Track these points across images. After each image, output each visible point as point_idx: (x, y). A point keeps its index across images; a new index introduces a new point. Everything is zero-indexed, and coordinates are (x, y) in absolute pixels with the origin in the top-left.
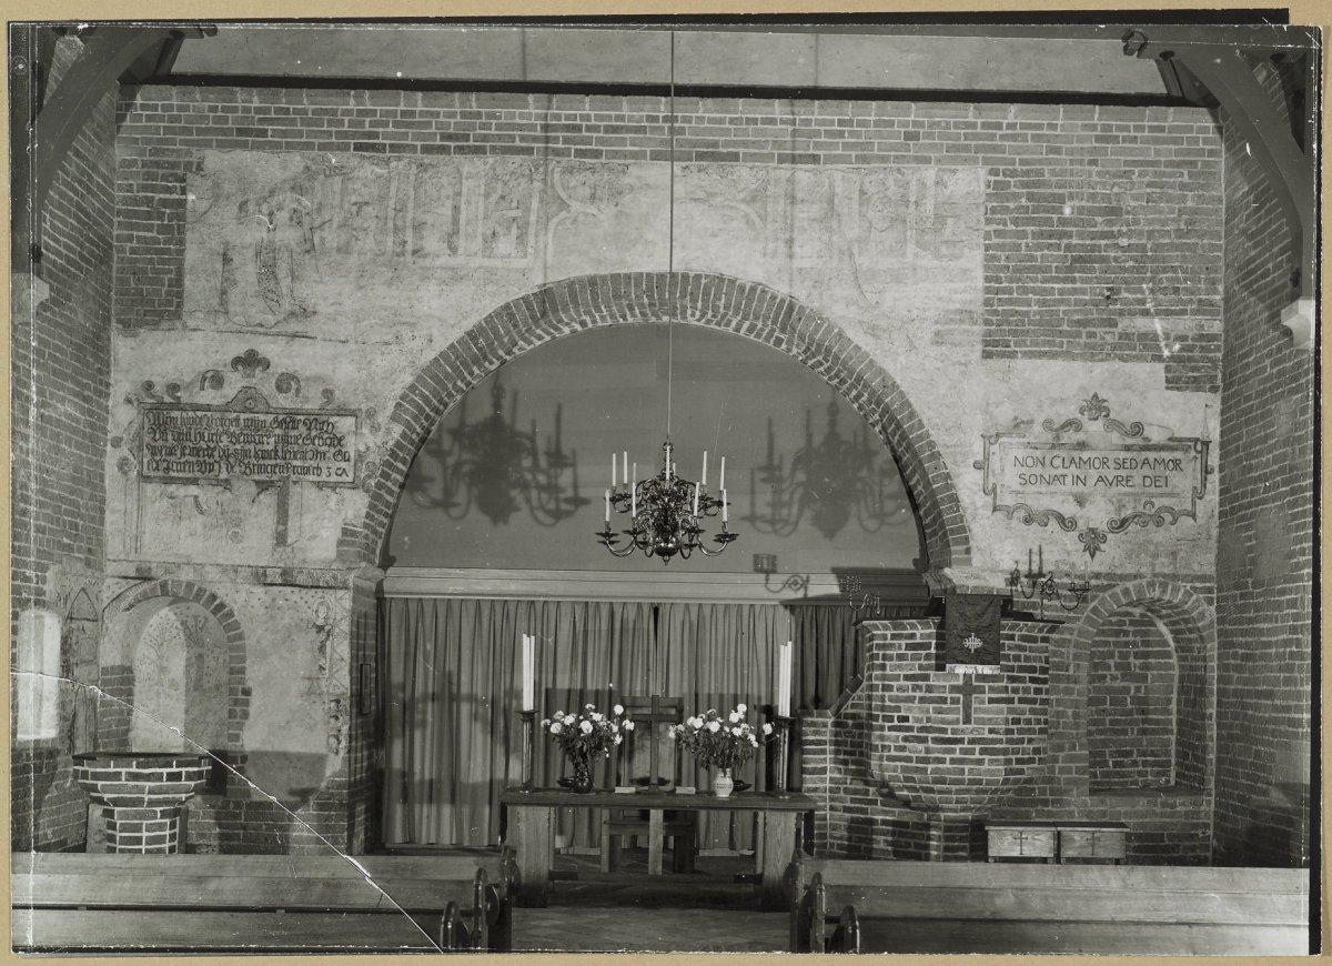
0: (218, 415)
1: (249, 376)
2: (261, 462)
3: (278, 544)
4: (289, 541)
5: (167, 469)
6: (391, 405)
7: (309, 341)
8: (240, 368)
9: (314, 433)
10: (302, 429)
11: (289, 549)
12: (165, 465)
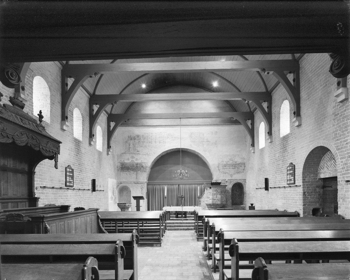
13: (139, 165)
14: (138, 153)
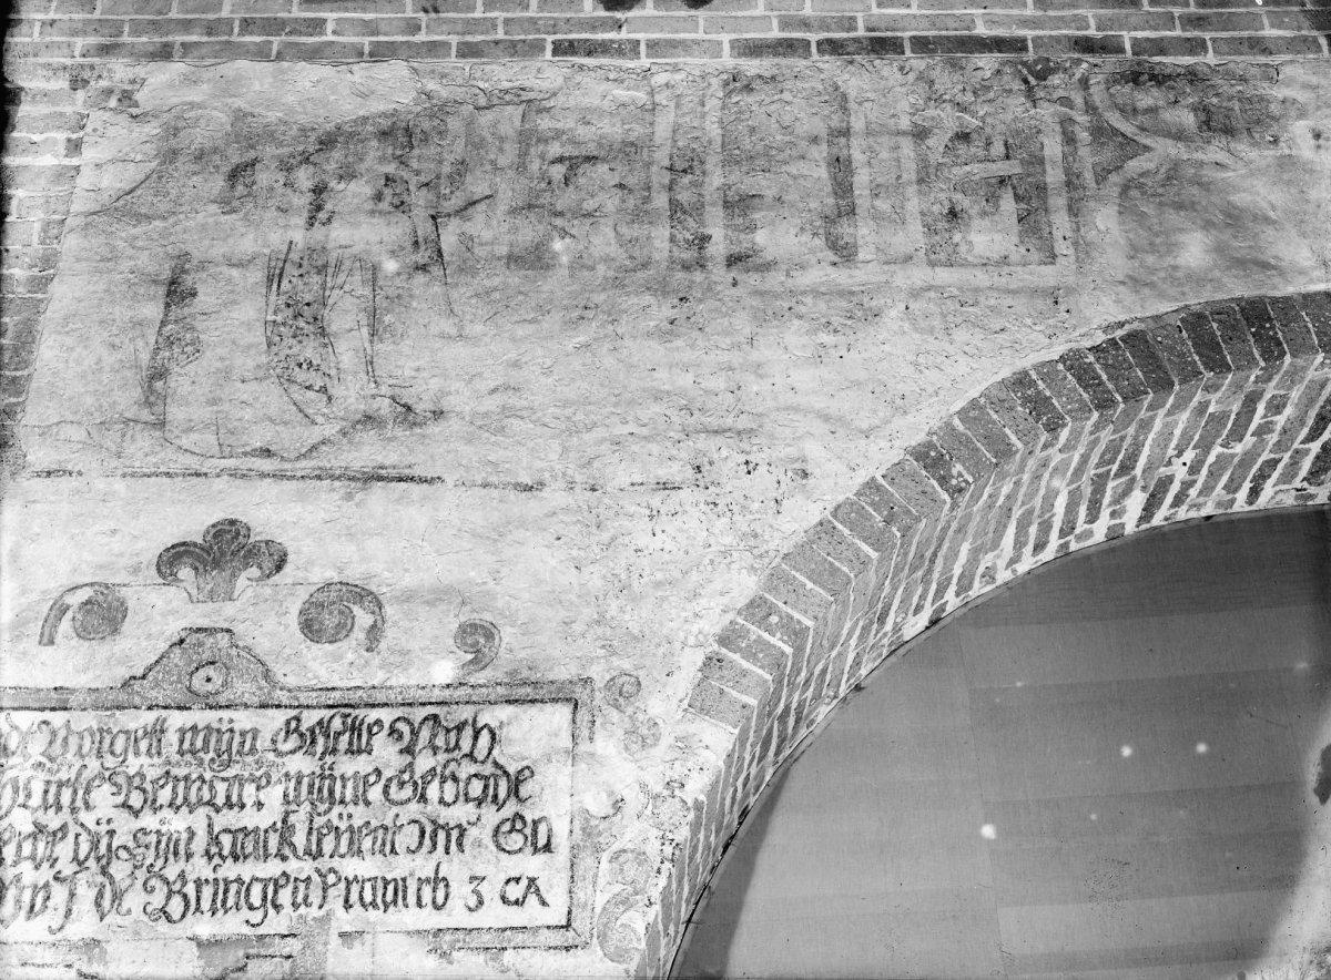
0: (88, 720)
1: (212, 596)
2: (230, 870)
6: (691, 660)
8: (185, 573)
9: (424, 762)
10: (385, 753)
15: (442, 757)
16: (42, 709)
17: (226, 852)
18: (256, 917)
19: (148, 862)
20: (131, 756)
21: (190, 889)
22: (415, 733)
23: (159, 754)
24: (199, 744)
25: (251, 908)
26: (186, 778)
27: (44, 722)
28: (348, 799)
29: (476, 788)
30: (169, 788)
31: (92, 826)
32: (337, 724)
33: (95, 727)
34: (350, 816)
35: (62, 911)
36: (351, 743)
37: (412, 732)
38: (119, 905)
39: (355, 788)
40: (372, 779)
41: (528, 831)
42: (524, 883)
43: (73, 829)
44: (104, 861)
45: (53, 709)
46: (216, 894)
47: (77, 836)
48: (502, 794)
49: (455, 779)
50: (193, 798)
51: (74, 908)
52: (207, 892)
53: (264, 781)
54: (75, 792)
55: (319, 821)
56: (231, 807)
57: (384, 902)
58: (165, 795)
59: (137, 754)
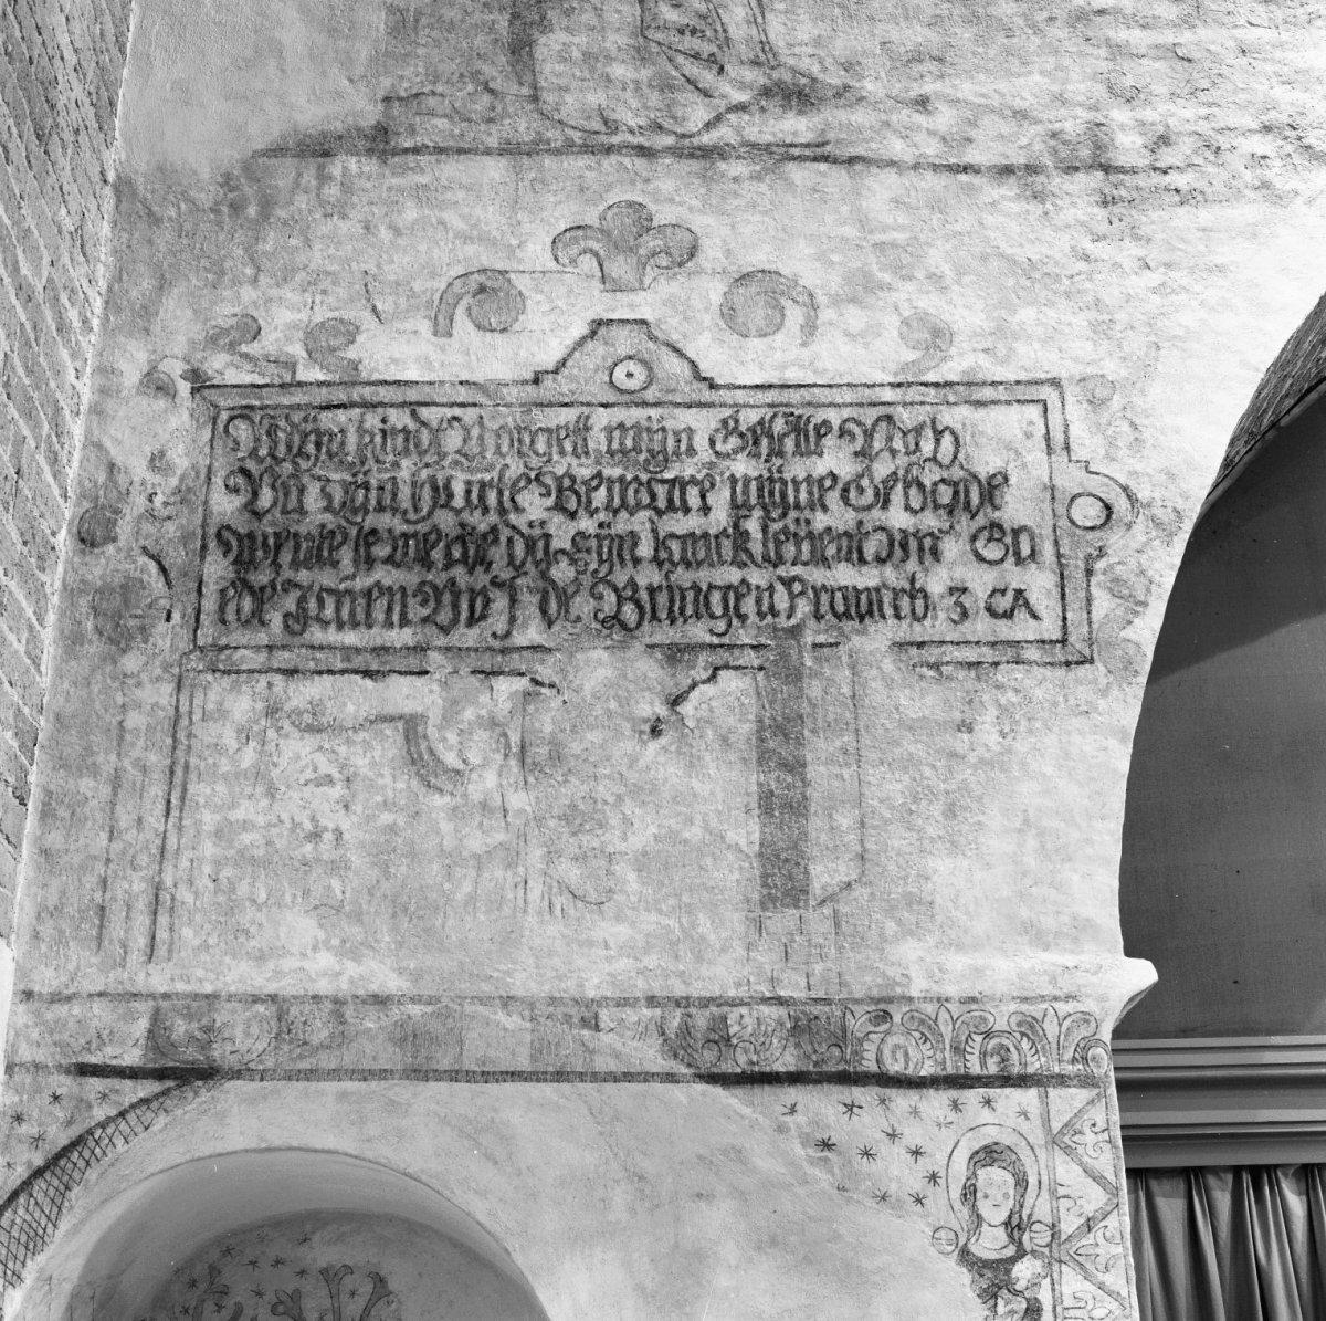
2: (683, 577)
3: (769, 901)
4: (816, 887)
5: (297, 622)
7: (835, 178)
9: (882, 469)
11: (818, 922)
12: (290, 603)
13: (835, 460)
14: (796, 126)
15: (902, 461)
16: (452, 405)
17: (677, 557)
18: (721, 626)
19: (593, 566)
20: (555, 457)
21: (644, 596)
22: (869, 435)
23: (587, 453)
24: (629, 443)
25: (713, 616)
26: (622, 479)
27: (455, 418)
28: (803, 504)
29: (945, 495)
30: (603, 491)
31: (525, 529)
32: (779, 426)
33: (511, 424)
34: (808, 522)
35: (504, 618)
36: (798, 445)
37: (865, 432)
38: (567, 611)
39: (810, 493)
40: (828, 483)
41: (1008, 540)
42: (1010, 595)
43: (505, 533)
44: (543, 566)
45: (463, 405)
46: (672, 601)
47: (510, 540)
48: (975, 499)
49: (921, 486)
50: (631, 501)
51: (518, 613)
52: (662, 599)
53: (707, 484)
54: (500, 493)
55: (775, 527)
56: (675, 510)
57: (858, 611)
58: (600, 497)
59: (562, 453)
